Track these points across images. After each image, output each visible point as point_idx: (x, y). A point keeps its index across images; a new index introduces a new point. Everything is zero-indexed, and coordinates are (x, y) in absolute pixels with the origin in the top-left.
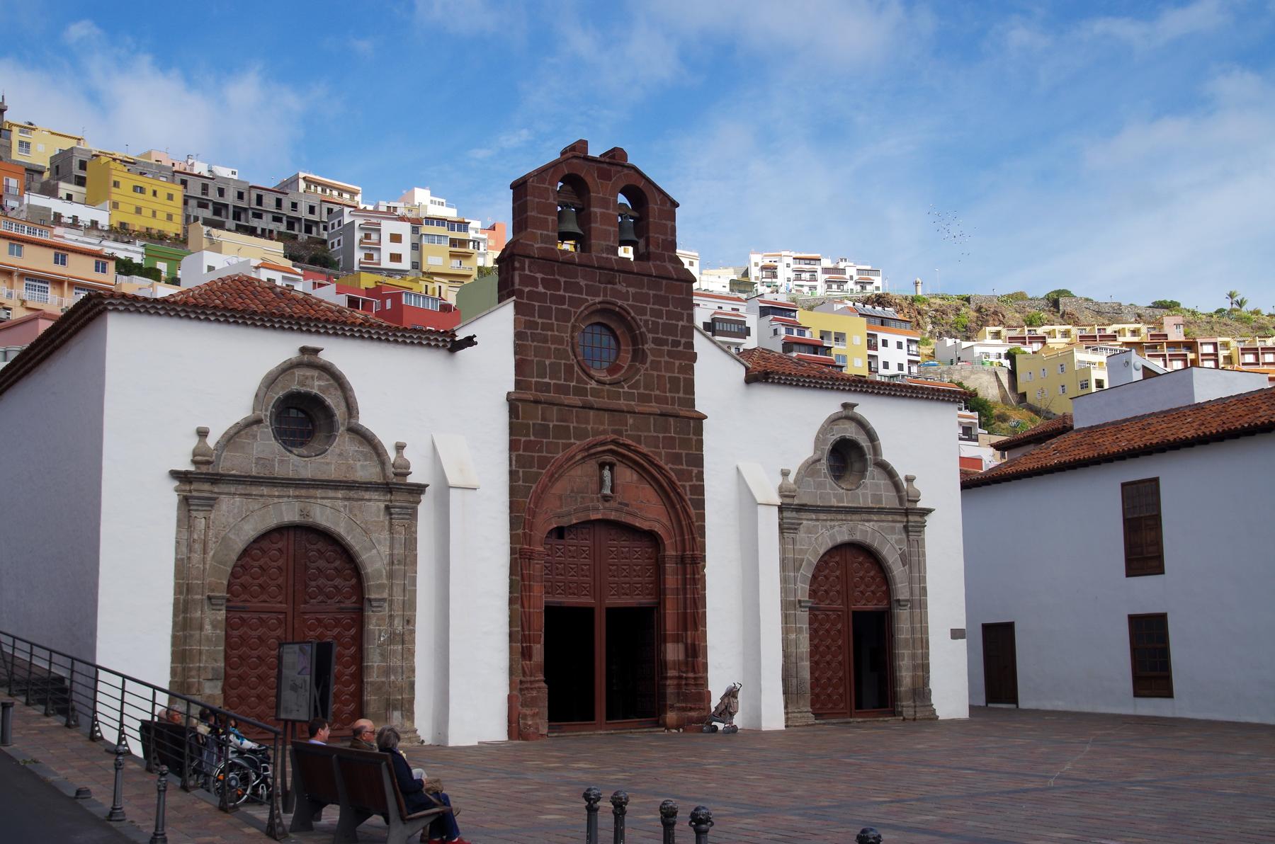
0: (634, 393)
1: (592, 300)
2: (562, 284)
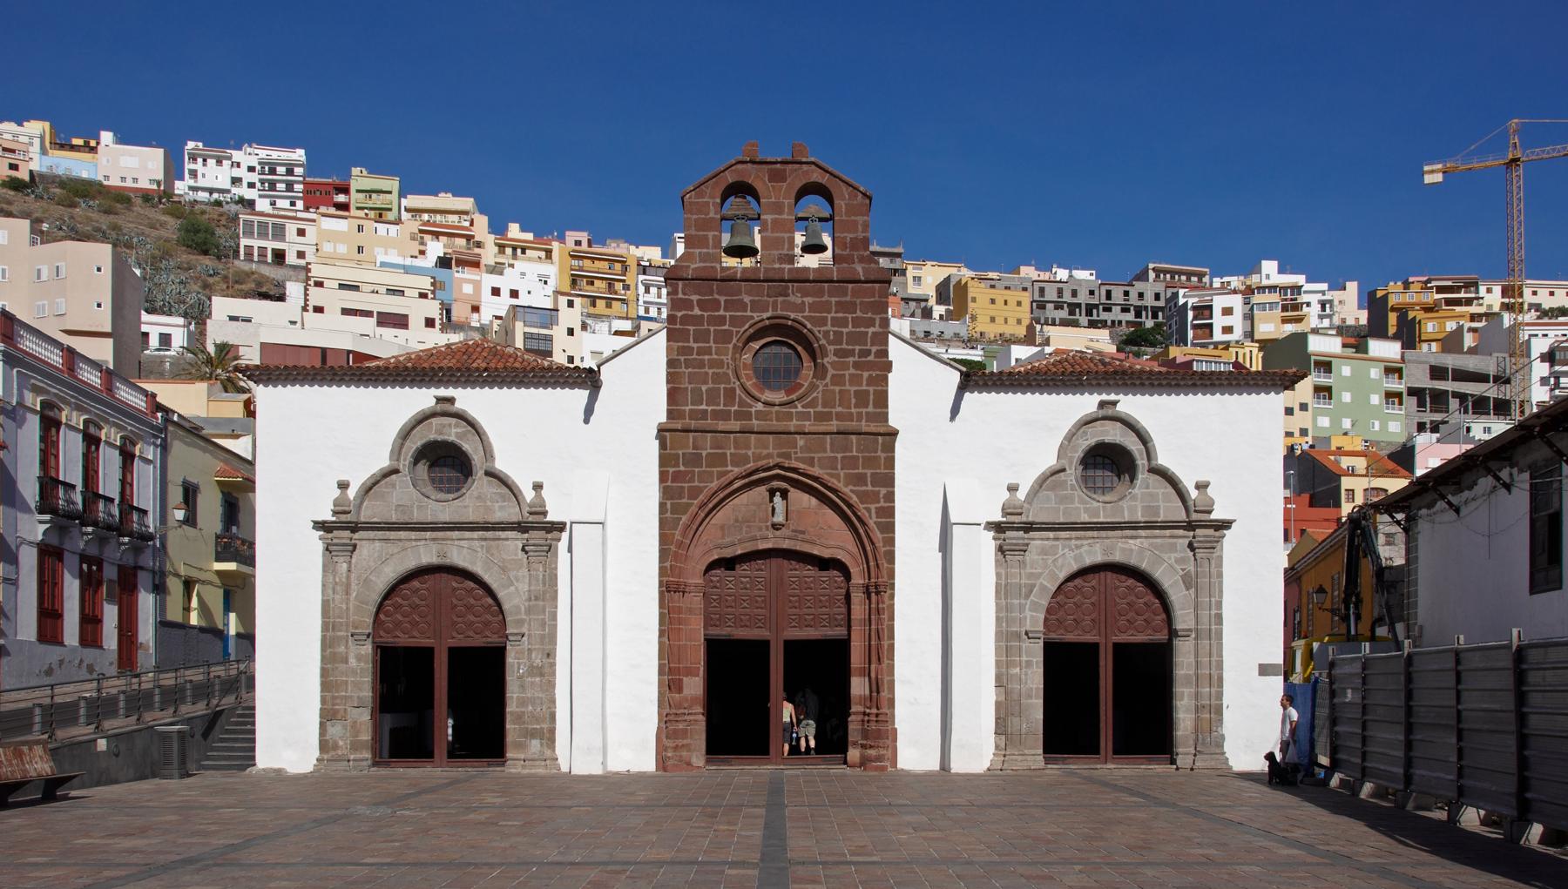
0: (810, 412)
2: (723, 303)
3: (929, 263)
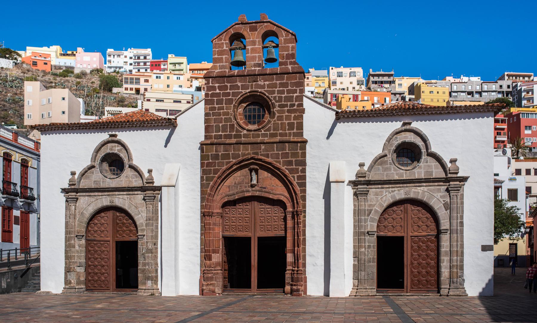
1: (244, 92)
2: (229, 87)
3: (405, 78)
